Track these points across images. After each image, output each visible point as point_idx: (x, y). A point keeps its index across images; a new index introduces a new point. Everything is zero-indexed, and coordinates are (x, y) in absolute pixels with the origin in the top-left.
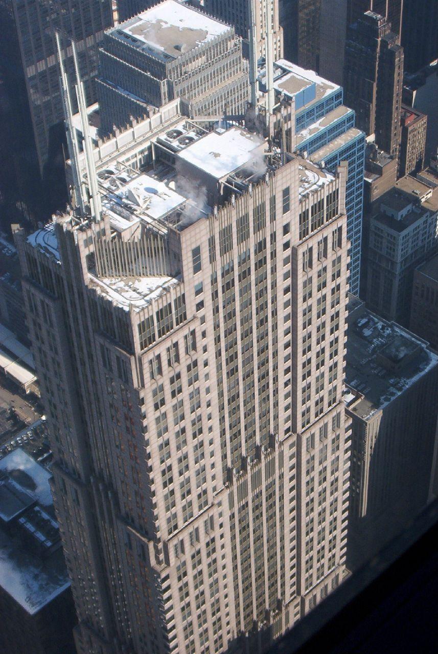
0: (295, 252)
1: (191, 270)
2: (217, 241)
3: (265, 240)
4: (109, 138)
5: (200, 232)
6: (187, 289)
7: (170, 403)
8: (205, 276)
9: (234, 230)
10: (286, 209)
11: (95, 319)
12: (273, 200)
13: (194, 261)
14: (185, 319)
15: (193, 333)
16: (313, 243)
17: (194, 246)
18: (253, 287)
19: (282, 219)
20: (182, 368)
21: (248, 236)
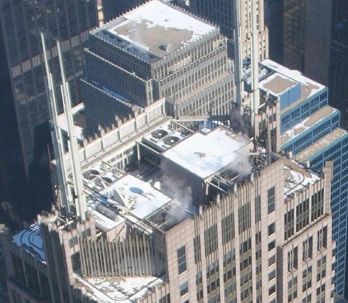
0: (280, 252)
1: (177, 270)
3: (250, 240)
4: (94, 138)
5: (185, 233)
6: (172, 289)
8: (190, 276)
9: (219, 230)
10: (271, 209)
12: (258, 200)
13: (179, 261)
16: (299, 243)
17: (179, 247)
18: (238, 287)
19: (267, 219)
21: (233, 236)
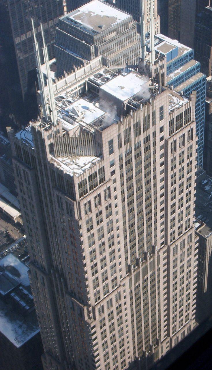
1: (108, 153)
2: (123, 136)
3: (150, 136)
4: (61, 78)
5: (113, 131)
6: (105, 163)
7: (96, 228)
8: (115, 156)
9: (132, 130)
10: (161, 118)
11: (54, 181)
12: (154, 113)
13: (110, 148)
14: (105, 180)
15: (109, 188)
16: (177, 137)
17: (109, 139)
18: (143, 163)
19: (159, 124)
20: (103, 208)
21: (140, 134)
